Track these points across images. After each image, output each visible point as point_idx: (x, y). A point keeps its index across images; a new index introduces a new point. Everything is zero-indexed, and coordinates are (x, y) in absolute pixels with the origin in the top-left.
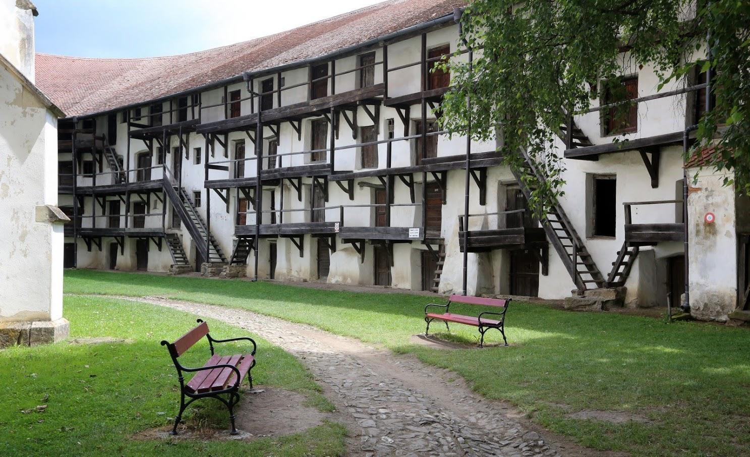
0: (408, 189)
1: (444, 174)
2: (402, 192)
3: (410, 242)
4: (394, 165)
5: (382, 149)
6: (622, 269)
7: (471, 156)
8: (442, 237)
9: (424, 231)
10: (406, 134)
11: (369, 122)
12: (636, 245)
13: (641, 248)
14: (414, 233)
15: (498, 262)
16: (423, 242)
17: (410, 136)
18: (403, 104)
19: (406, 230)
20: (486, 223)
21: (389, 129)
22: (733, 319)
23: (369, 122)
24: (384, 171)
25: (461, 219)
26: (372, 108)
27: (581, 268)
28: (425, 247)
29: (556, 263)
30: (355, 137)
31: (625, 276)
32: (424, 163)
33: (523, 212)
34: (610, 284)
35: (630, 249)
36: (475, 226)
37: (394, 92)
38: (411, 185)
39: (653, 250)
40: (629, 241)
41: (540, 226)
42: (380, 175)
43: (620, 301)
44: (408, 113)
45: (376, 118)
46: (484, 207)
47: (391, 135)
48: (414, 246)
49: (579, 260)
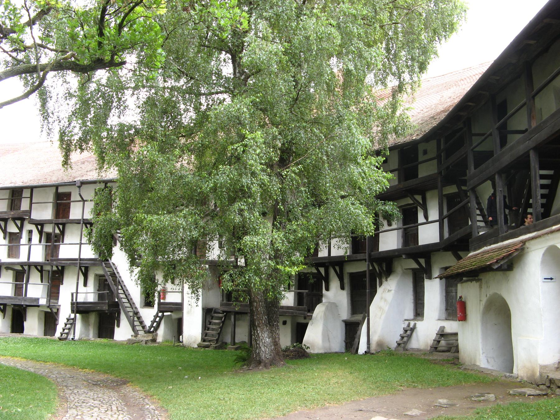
0: (39, 274)
1: (63, 268)
2: (35, 277)
3: (38, 306)
4: (32, 260)
5: (24, 250)
6: (155, 324)
7: (81, 260)
8: (59, 304)
9: (49, 301)
10: (40, 241)
11: (17, 231)
12: (163, 312)
13: (165, 314)
14: (43, 302)
15: (93, 318)
16: (48, 307)
17: (42, 243)
18: (40, 224)
19: (37, 300)
20: (86, 297)
21: (29, 236)
22: (199, 346)
23: (17, 231)
24: (25, 263)
25: (72, 294)
26: (19, 222)
27: (137, 323)
28: (49, 310)
29: (124, 321)
30: (5, 238)
31: (157, 328)
32: (52, 260)
33: (108, 293)
34: (149, 332)
35: (160, 314)
36: (81, 299)
37: (36, 215)
38: (41, 271)
39: (171, 315)
40: (160, 310)
41: (116, 300)
42: (22, 264)
43: (154, 340)
44: (42, 228)
45: (21, 229)
46: (85, 288)
47: (30, 240)
48: (40, 309)
49: (136, 319)
